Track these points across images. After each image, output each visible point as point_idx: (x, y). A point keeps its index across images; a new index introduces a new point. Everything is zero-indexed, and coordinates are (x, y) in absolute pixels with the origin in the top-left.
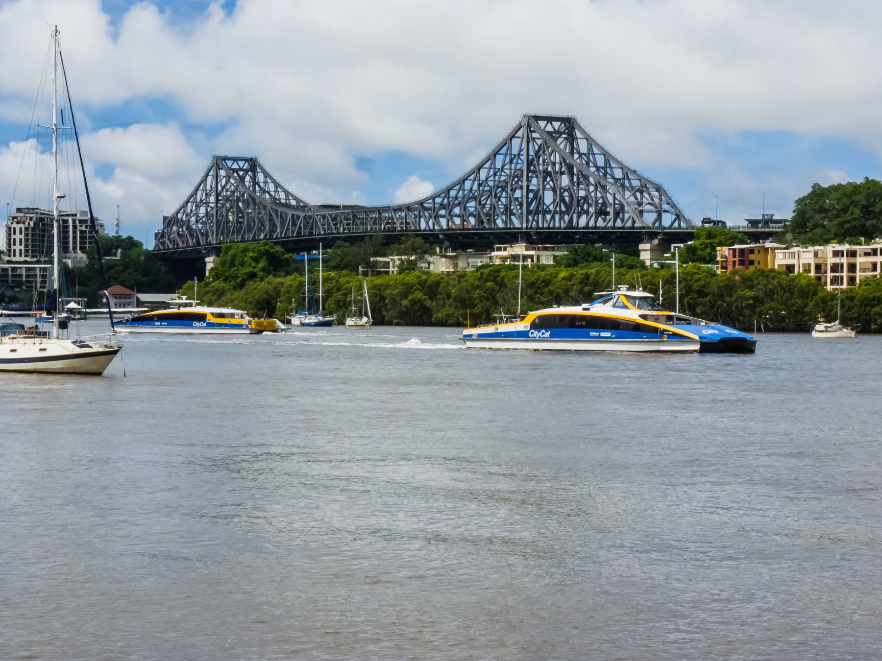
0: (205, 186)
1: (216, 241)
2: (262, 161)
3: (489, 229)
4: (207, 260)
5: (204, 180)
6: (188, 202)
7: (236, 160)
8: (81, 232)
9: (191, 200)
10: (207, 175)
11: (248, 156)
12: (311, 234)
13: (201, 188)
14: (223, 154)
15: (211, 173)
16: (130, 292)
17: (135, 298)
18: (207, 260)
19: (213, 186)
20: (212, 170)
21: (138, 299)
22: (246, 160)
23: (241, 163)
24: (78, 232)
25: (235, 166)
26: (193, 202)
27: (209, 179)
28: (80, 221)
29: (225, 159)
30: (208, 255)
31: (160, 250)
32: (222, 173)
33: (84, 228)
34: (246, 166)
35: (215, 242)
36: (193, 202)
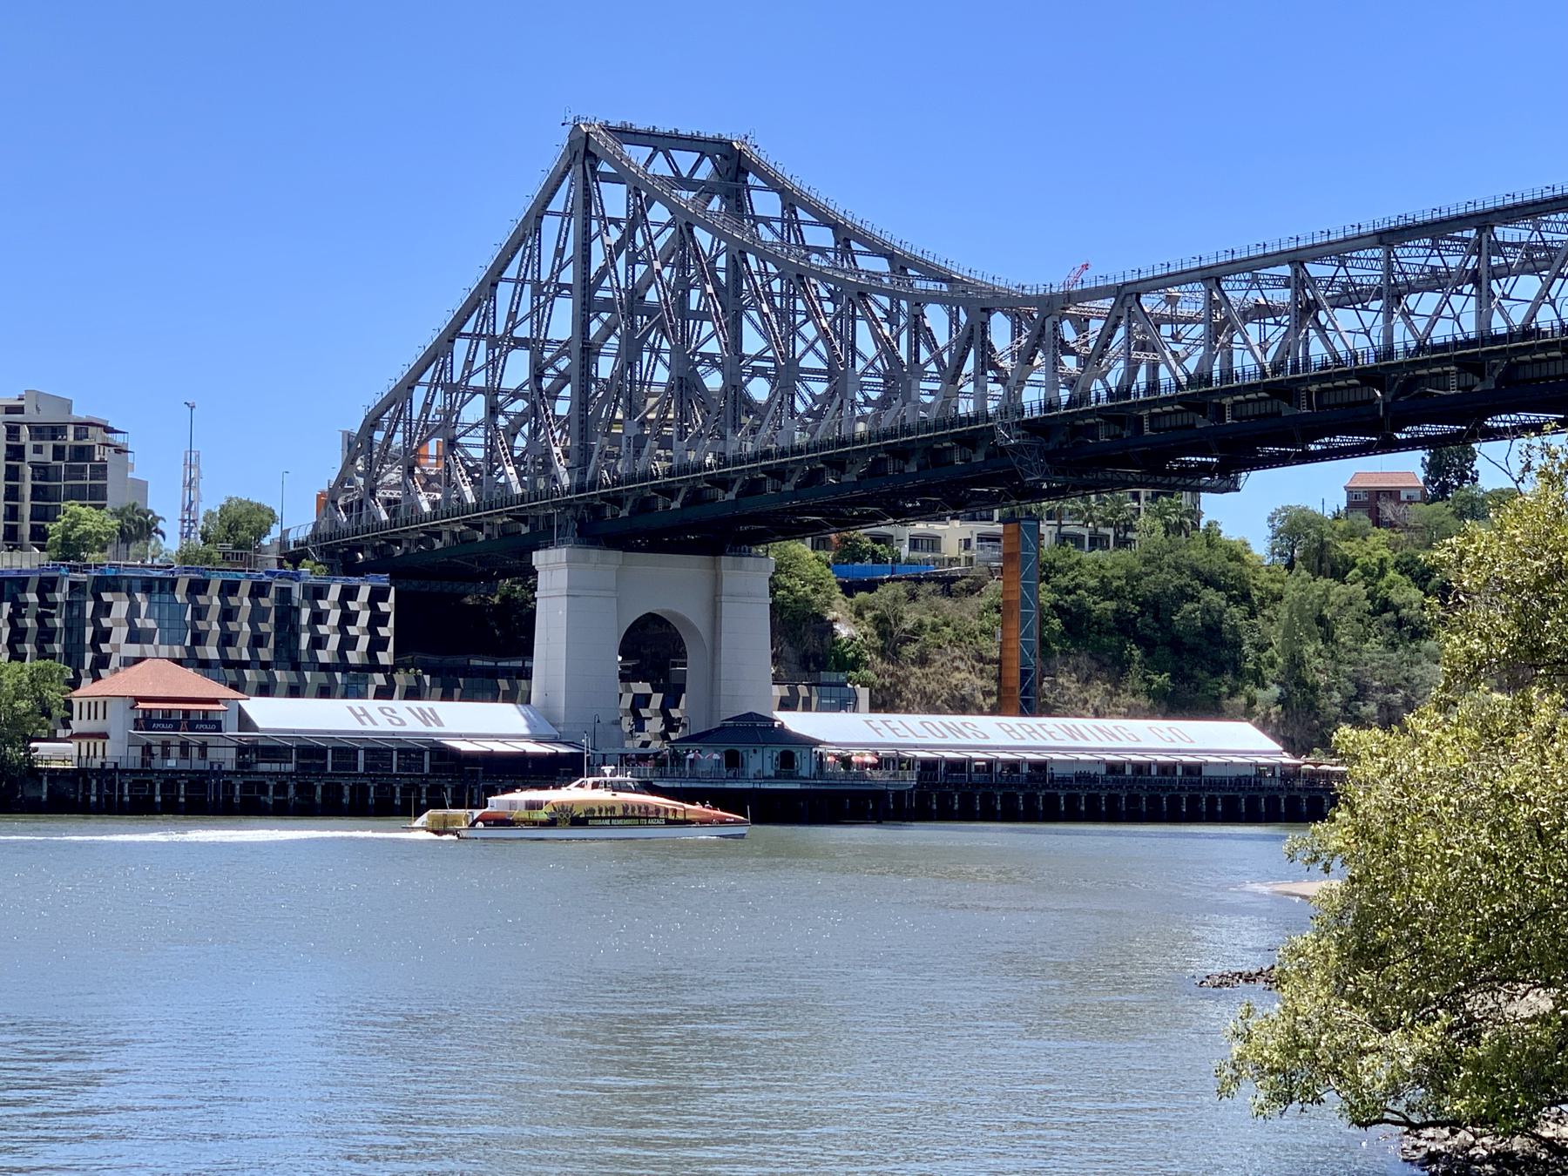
0: (534, 258)
2: (767, 150)
4: (539, 558)
6: (453, 332)
7: (662, 142)
8: (41, 471)
9: (468, 328)
10: (540, 210)
11: (710, 133)
13: (511, 272)
15: (557, 204)
18: (539, 558)
19: (569, 253)
20: (567, 180)
23: (685, 160)
24: (28, 471)
25: (660, 167)
27: (550, 226)
28: (38, 431)
32: (615, 200)
33: (47, 456)
34: (705, 171)
36: (476, 337)
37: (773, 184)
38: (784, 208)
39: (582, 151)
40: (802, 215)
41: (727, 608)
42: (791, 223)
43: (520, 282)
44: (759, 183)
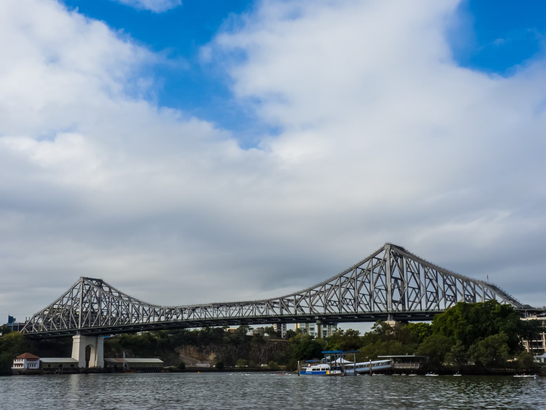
1: (81, 326)
3: (29, 333)
4: (74, 337)
5: (71, 291)
7: (92, 280)
12: (88, 326)
13: (68, 296)
14: (86, 276)
15: (78, 287)
16: (35, 357)
17: (38, 362)
18: (74, 337)
21: (40, 362)
22: (97, 280)
23: (94, 282)
26: (60, 304)
29: (87, 279)
30: (75, 334)
31: (26, 332)
35: (79, 327)
37: (107, 286)
38: (109, 289)
39: (82, 281)
40: (112, 291)
41: (98, 344)
42: (110, 291)
43: (69, 297)
44: (105, 286)
